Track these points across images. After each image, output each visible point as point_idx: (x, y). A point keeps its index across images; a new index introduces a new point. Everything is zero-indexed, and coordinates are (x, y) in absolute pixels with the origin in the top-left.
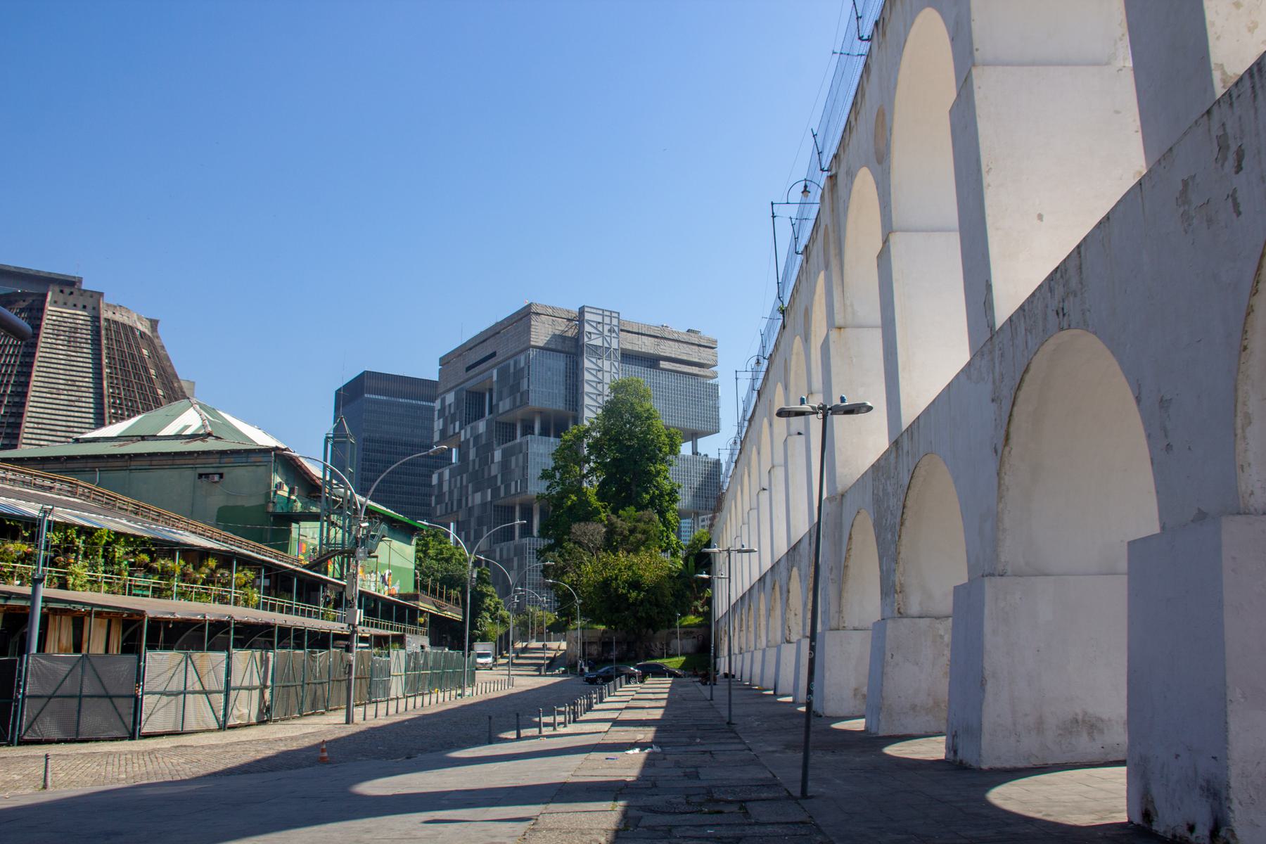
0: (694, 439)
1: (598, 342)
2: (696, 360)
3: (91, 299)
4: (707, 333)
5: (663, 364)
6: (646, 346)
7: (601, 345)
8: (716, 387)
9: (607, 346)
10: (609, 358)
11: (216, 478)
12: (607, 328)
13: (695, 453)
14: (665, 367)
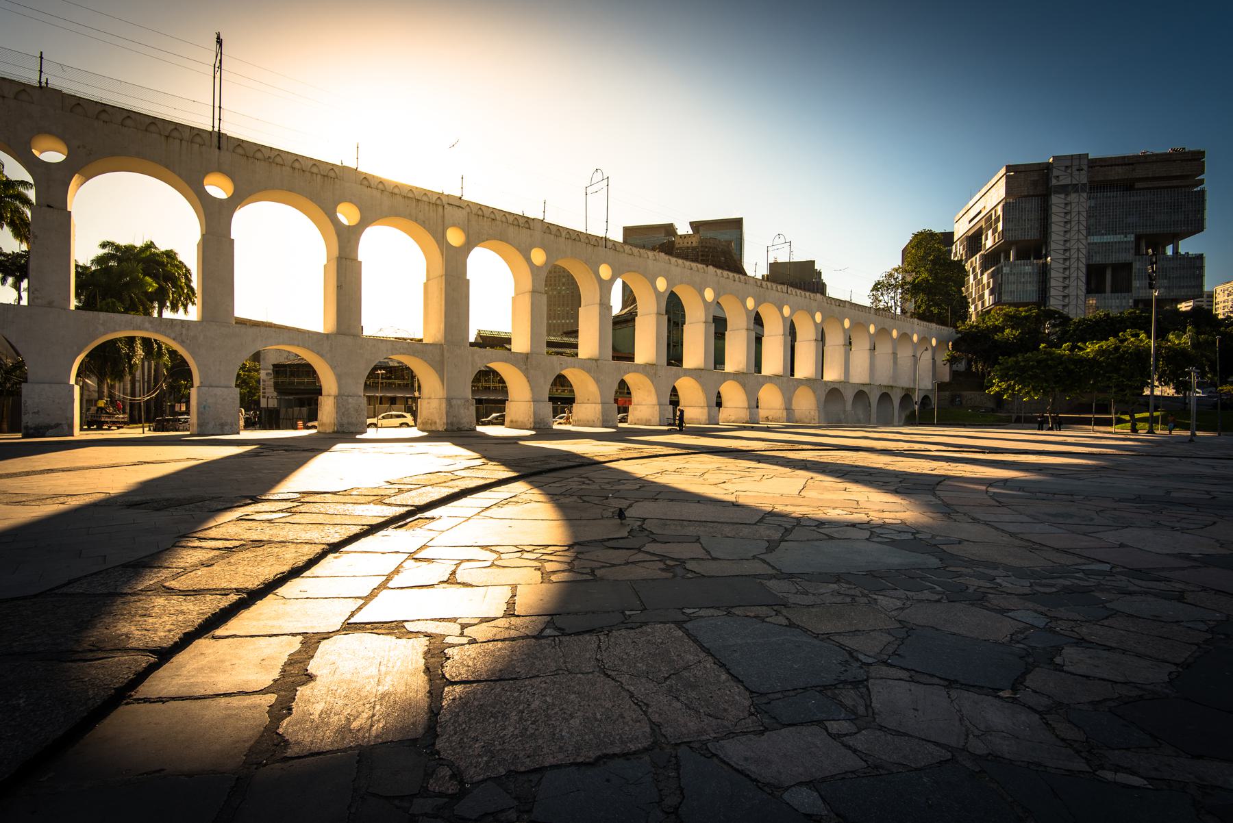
0: (1175, 241)
1: (1065, 181)
2: (1178, 174)
4: (1191, 147)
5: (1138, 185)
6: (1117, 173)
7: (1070, 183)
8: (1203, 192)
9: (1077, 183)
10: (1077, 191)
12: (1075, 168)
13: (1176, 251)
14: (1141, 187)
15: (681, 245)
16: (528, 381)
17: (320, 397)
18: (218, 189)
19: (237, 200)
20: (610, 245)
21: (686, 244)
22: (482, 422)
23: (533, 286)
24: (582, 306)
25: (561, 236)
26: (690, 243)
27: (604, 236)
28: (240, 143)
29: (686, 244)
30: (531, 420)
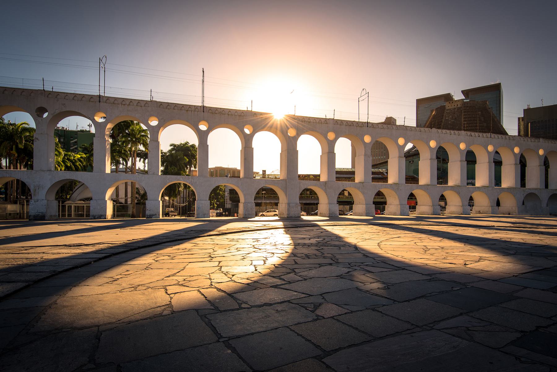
3: (459, 102)
11: (412, 162)
15: (450, 107)
16: (326, 194)
17: (239, 203)
18: (203, 127)
19: (210, 129)
20: (369, 125)
21: (453, 106)
22: (311, 214)
23: (329, 150)
24: (357, 156)
25: (343, 125)
26: (456, 105)
27: (367, 121)
28: (210, 108)
29: (453, 107)
30: (328, 213)
